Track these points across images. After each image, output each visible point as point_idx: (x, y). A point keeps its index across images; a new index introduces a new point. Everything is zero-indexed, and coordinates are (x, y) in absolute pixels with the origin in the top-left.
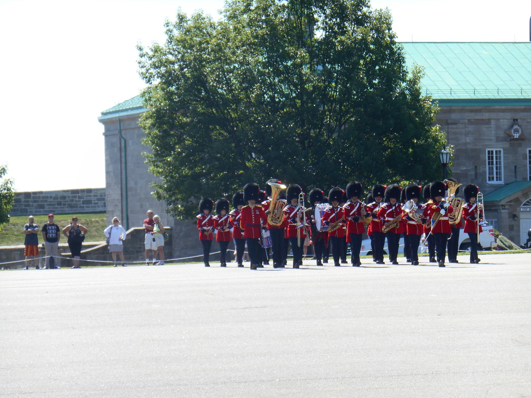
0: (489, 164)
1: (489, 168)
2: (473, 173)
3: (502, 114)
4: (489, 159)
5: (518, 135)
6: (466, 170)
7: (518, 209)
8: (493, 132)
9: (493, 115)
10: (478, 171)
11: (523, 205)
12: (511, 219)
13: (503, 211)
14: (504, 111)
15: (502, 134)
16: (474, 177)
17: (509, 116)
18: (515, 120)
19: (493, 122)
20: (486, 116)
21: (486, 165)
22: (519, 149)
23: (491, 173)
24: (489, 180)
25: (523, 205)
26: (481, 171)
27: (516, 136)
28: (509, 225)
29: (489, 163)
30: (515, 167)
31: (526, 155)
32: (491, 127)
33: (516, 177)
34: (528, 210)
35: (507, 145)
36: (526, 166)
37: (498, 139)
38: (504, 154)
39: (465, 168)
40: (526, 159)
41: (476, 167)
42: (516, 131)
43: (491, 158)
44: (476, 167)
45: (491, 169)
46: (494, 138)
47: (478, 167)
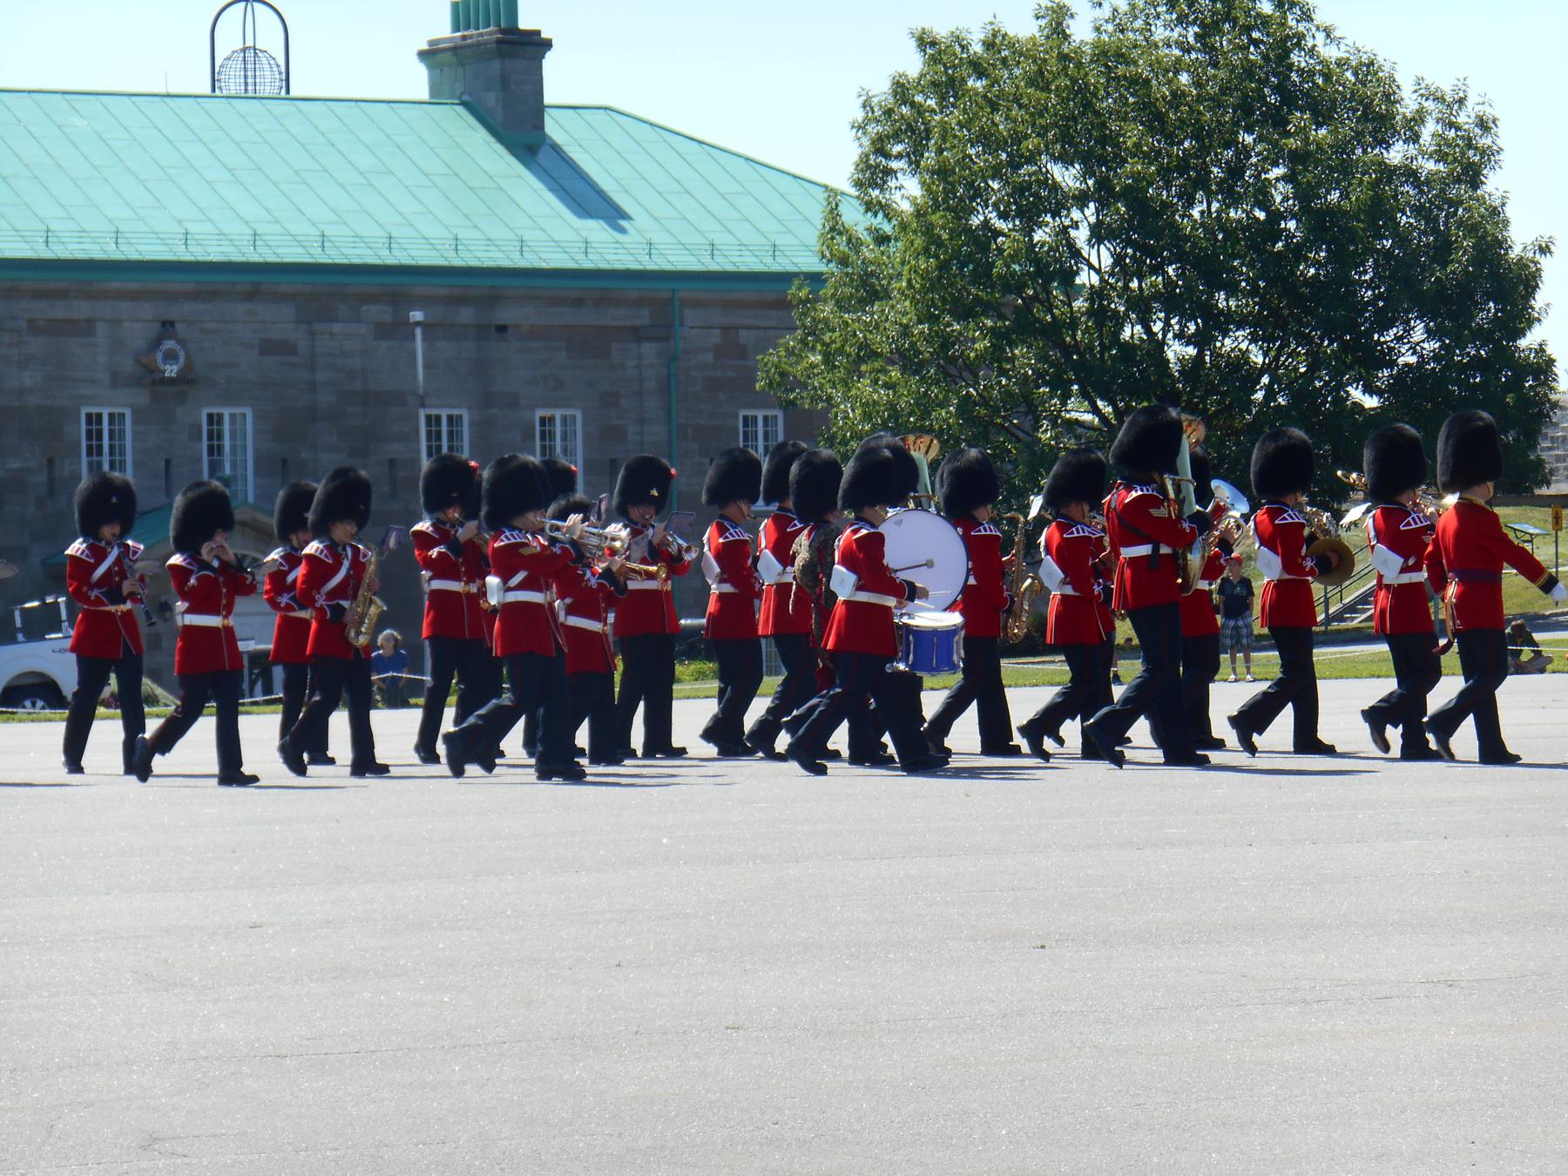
0: (90, 453)
1: (90, 464)
2: (41, 478)
3: (128, 305)
5: (175, 368)
14: (135, 296)
15: (127, 365)
17: (148, 310)
19: (102, 330)
20: (81, 310)
27: (171, 370)
29: (90, 449)
30: (168, 462)
31: (200, 427)
35: (142, 397)
36: (199, 460)
37: (116, 381)
38: (134, 422)
40: (200, 439)
41: (51, 462)
42: (171, 356)
43: (94, 435)
44: (51, 462)
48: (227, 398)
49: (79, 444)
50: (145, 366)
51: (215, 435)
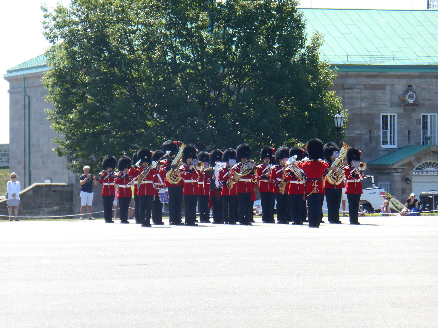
0: (383, 129)
1: (383, 132)
2: (367, 137)
3: (397, 80)
4: (383, 123)
5: (412, 100)
6: (361, 134)
7: (411, 172)
8: (388, 98)
9: (389, 81)
10: (372, 135)
11: (416, 169)
12: (403, 183)
13: (395, 174)
14: (399, 77)
15: (396, 99)
16: (368, 141)
17: (404, 82)
18: (410, 86)
19: (388, 88)
20: (381, 81)
21: (380, 129)
22: (413, 114)
23: (385, 137)
24: (383, 144)
25: (416, 169)
26: (375, 135)
27: (411, 101)
28: (402, 189)
29: (383, 127)
30: (409, 131)
32: (386, 93)
33: (409, 142)
34: (420, 173)
35: (401, 110)
36: (420, 131)
37: (393, 105)
38: (398, 118)
39: (359, 132)
40: (420, 124)
41: (370, 131)
42: (411, 97)
44: (370, 131)
45: (385, 134)
46: (389, 104)
47: (372, 131)
48: (429, 111)
49: (380, 125)
50: (402, 100)
51: (425, 123)
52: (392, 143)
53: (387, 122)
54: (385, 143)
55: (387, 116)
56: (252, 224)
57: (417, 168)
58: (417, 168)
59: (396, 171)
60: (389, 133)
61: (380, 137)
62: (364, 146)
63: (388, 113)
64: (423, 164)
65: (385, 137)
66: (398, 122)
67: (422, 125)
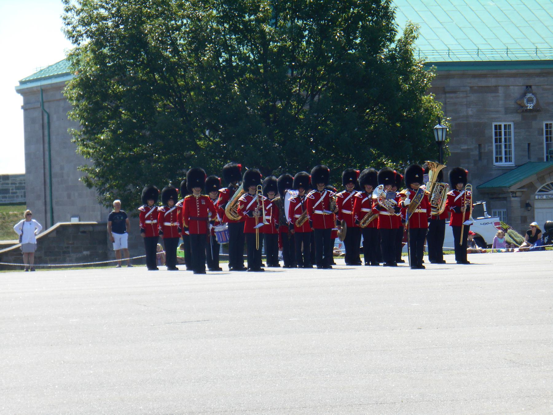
0: (496, 142)
1: (496, 146)
2: (476, 152)
3: (512, 79)
4: (496, 135)
5: (532, 105)
6: (468, 149)
7: (532, 196)
8: (501, 102)
9: (501, 81)
10: (483, 151)
11: (539, 192)
13: (513, 199)
14: (515, 76)
15: (512, 104)
16: (478, 158)
17: (520, 81)
18: (529, 87)
19: (501, 90)
20: (492, 82)
23: (499, 152)
25: (539, 192)
26: (486, 151)
27: (530, 106)
28: (522, 217)
29: (496, 140)
30: (529, 144)
33: (529, 158)
34: (544, 197)
35: (518, 118)
36: (542, 144)
37: (507, 111)
38: (515, 128)
39: (466, 147)
40: (542, 134)
41: (480, 145)
42: (530, 100)
44: (480, 145)
45: (498, 148)
47: (483, 145)
49: (492, 137)
50: (520, 105)
52: (508, 159)
53: (500, 133)
54: (499, 159)
55: (500, 126)
56: (333, 266)
57: (540, 191)
58: (540, 191)
59: (514, 195)
60: (503, 147)
61: (492, 152)
62: (472, 165)
63: (500, 121)
64: (548, 185)
65: (499, 152)
66: (515, 133)
67: (545, 136)
